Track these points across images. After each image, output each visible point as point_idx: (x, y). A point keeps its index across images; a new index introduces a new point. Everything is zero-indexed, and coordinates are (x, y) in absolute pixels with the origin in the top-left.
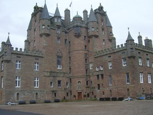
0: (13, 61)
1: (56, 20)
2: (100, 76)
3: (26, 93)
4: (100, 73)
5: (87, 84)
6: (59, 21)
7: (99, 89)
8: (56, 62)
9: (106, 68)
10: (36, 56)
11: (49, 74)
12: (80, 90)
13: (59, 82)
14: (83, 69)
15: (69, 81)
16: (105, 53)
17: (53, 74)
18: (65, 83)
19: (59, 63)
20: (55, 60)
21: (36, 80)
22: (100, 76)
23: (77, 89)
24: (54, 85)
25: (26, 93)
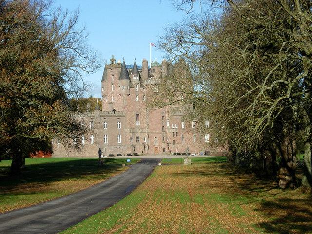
0: (102, 123)
1: (134, 78)
2: (175, 133)
3: (112, 148)
4: (175, 130)
5: (163, 140)
6: (138, 78)
7: (174, 144)
8: (135, 120)
9: (180, 127)
10: (119, 116)
11: (129, 131)
12: (156, 145)
13: (138, 138)
14: (160, 126)
15: (147, 136)
16: (180, 114)
17: (133, 130)
18: (143, 138)
19: (137, 119)
20: (134, 117)
21: (119, 137)
22: (175, 133)
23: (154, 144)
24: (133, 140)
25: (112, 148)
